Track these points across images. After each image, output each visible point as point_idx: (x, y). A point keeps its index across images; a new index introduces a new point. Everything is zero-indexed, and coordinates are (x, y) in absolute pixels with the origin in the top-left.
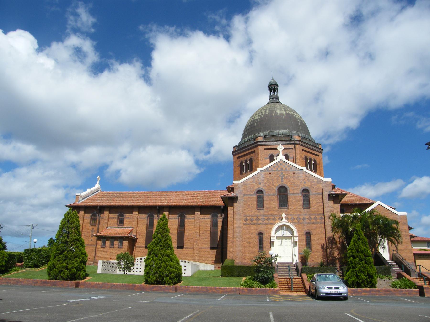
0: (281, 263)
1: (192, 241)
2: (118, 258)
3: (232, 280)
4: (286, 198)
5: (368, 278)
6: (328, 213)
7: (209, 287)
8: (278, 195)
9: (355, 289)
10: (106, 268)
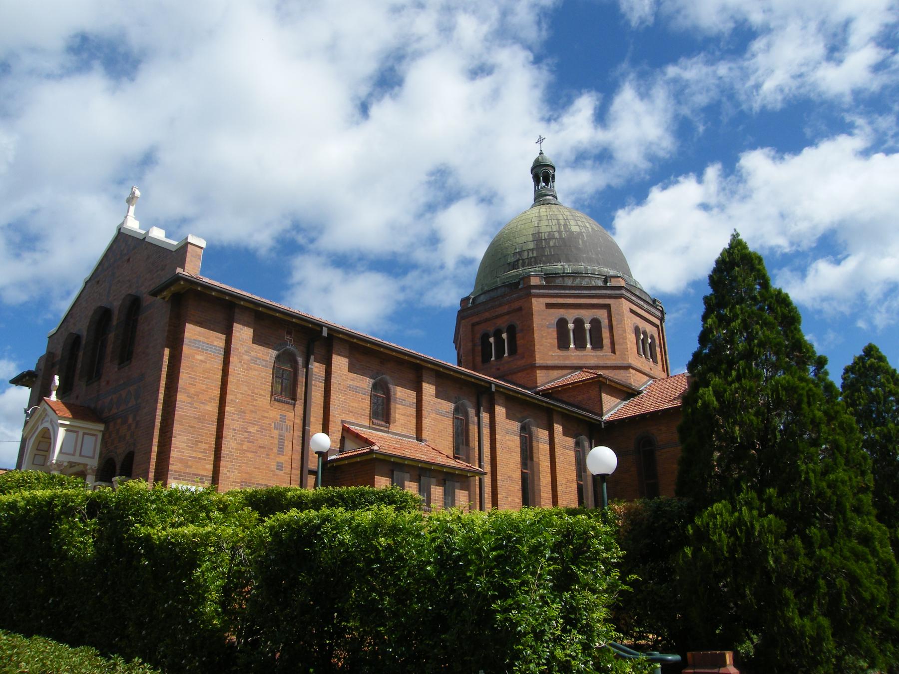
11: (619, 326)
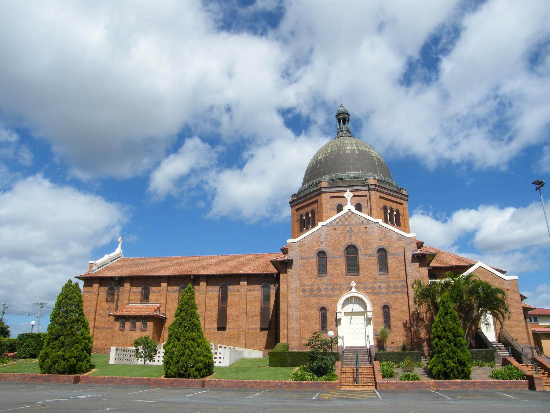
0: (350, 348)
1: (237, 320)
2: (137, 344)
3: (281, 371)
4: (356, 261)
5: (458, 366)
6: (411, 280)
7: (247, 380)
8: (345, 257)
9: (441, 381)
10: (122, 357)
11: (320, 211)
